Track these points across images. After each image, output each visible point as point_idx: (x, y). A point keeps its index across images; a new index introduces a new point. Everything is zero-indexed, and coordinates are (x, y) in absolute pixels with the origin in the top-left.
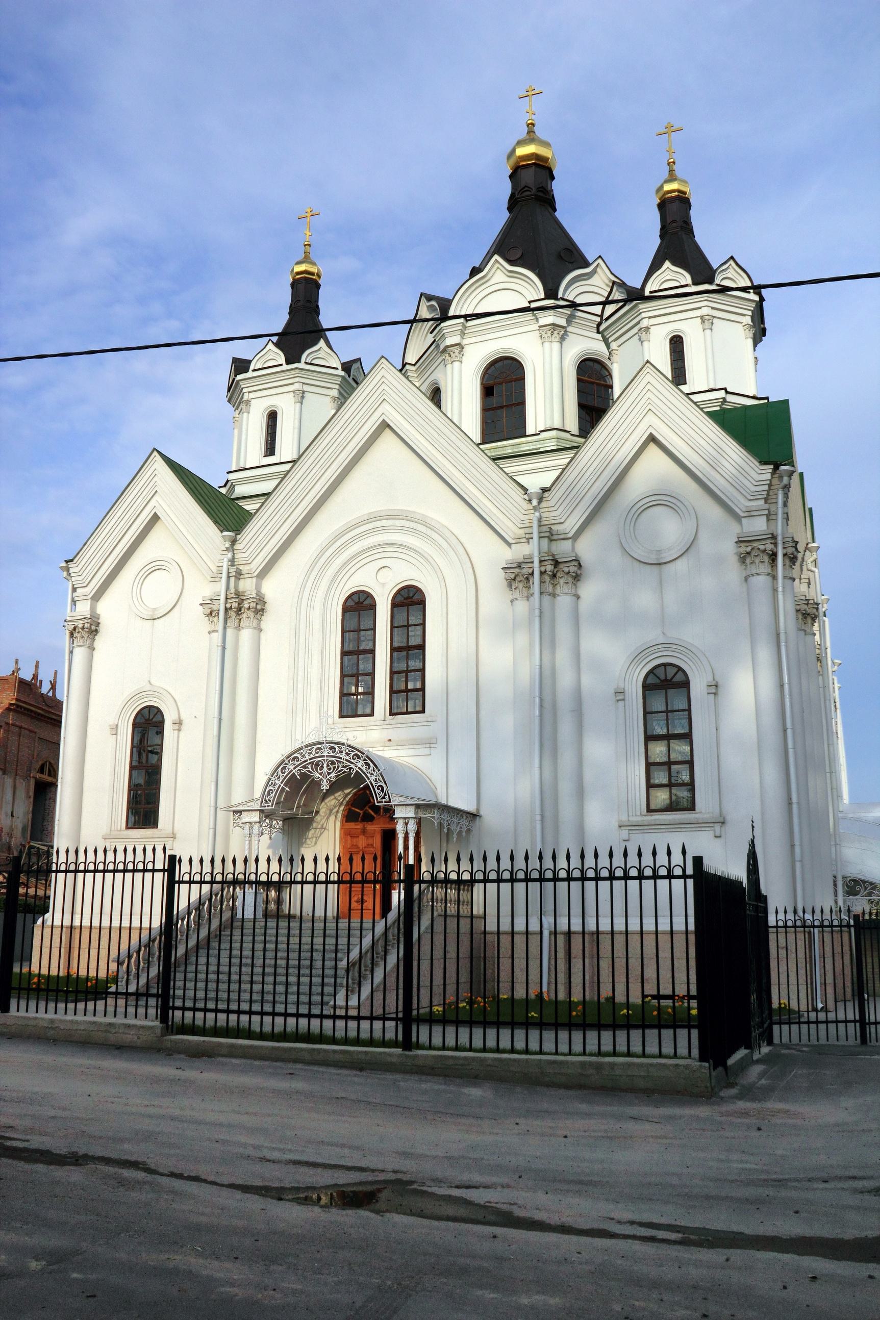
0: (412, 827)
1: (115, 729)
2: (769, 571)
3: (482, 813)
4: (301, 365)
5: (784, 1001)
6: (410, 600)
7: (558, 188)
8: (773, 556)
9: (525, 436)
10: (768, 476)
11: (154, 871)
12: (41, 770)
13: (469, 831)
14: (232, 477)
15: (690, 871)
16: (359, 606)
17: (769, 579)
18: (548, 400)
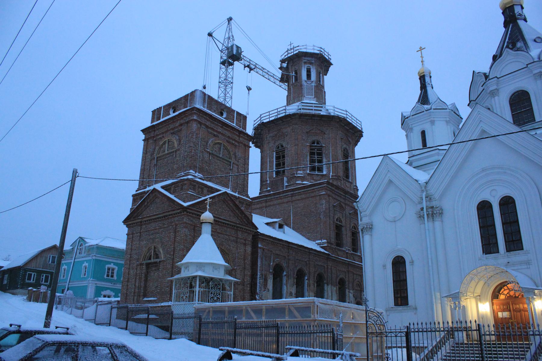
6: (508, 203)
14: (411, 159)
16: (484, 208)
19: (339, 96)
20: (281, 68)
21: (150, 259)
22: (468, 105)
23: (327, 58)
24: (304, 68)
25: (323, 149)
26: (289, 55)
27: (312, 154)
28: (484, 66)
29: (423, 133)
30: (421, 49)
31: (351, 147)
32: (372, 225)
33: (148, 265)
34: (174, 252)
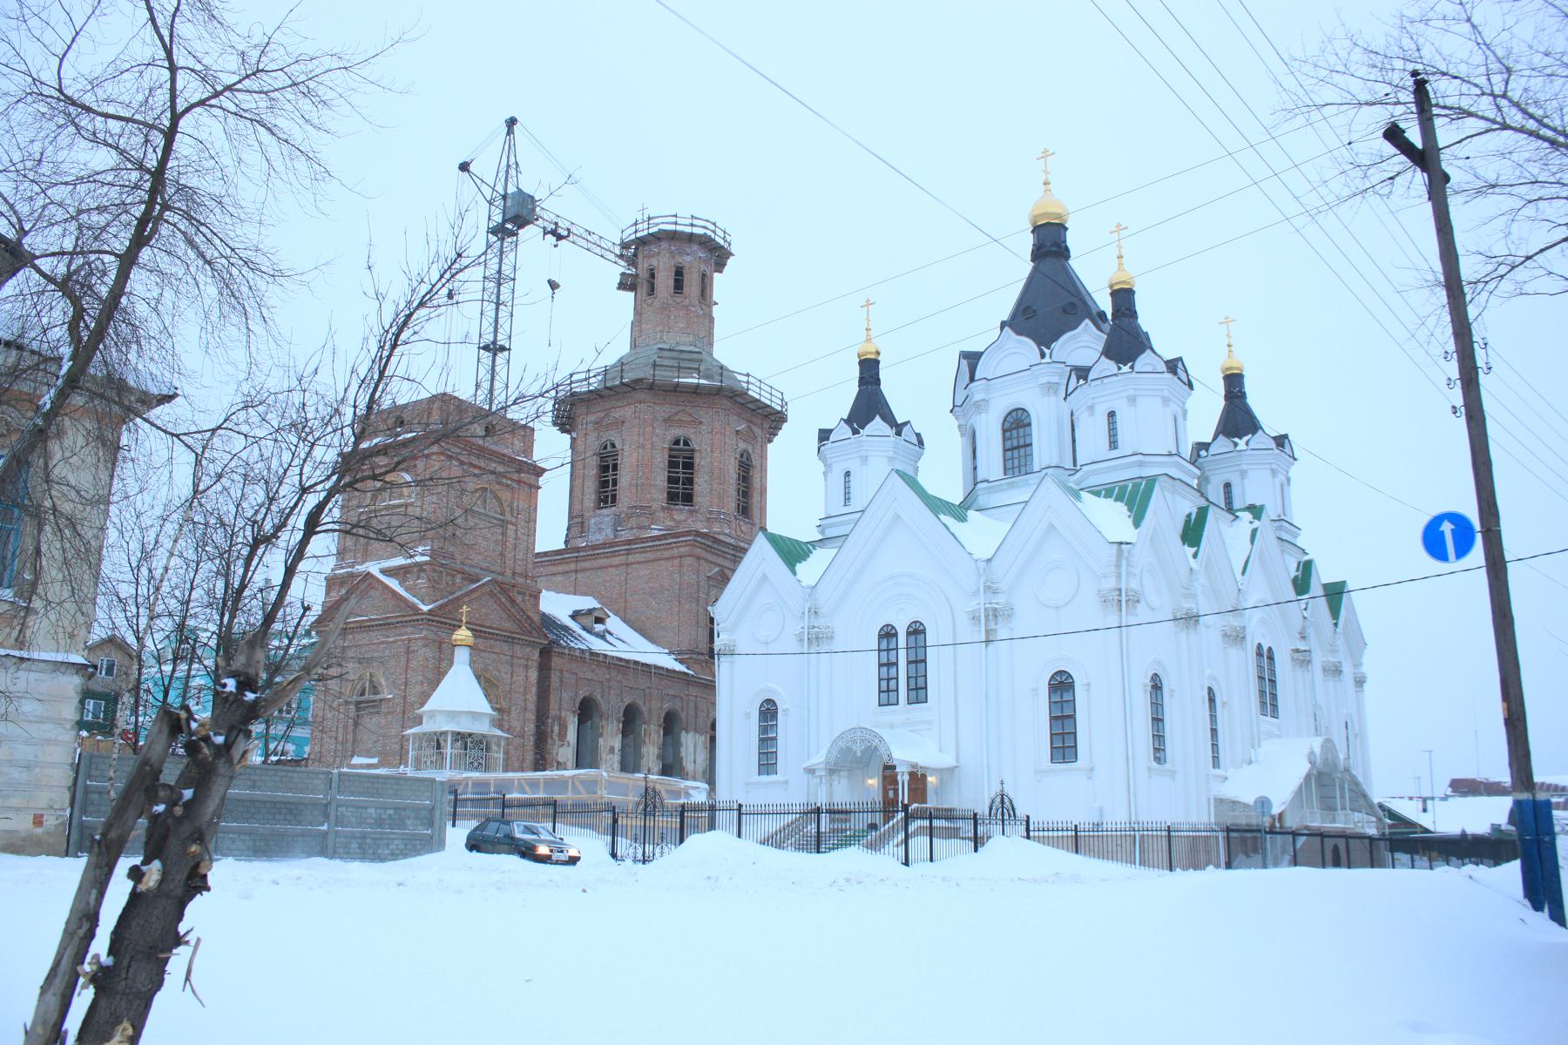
6: (916, 631)
7: (1072, 240)
16: (888, 634)
21: (363, 694)
23: (721, 242)
24: (672, 268)
25: (697, 455)
27: (672, 464)
33: (358, 703)
34: (406, 684)
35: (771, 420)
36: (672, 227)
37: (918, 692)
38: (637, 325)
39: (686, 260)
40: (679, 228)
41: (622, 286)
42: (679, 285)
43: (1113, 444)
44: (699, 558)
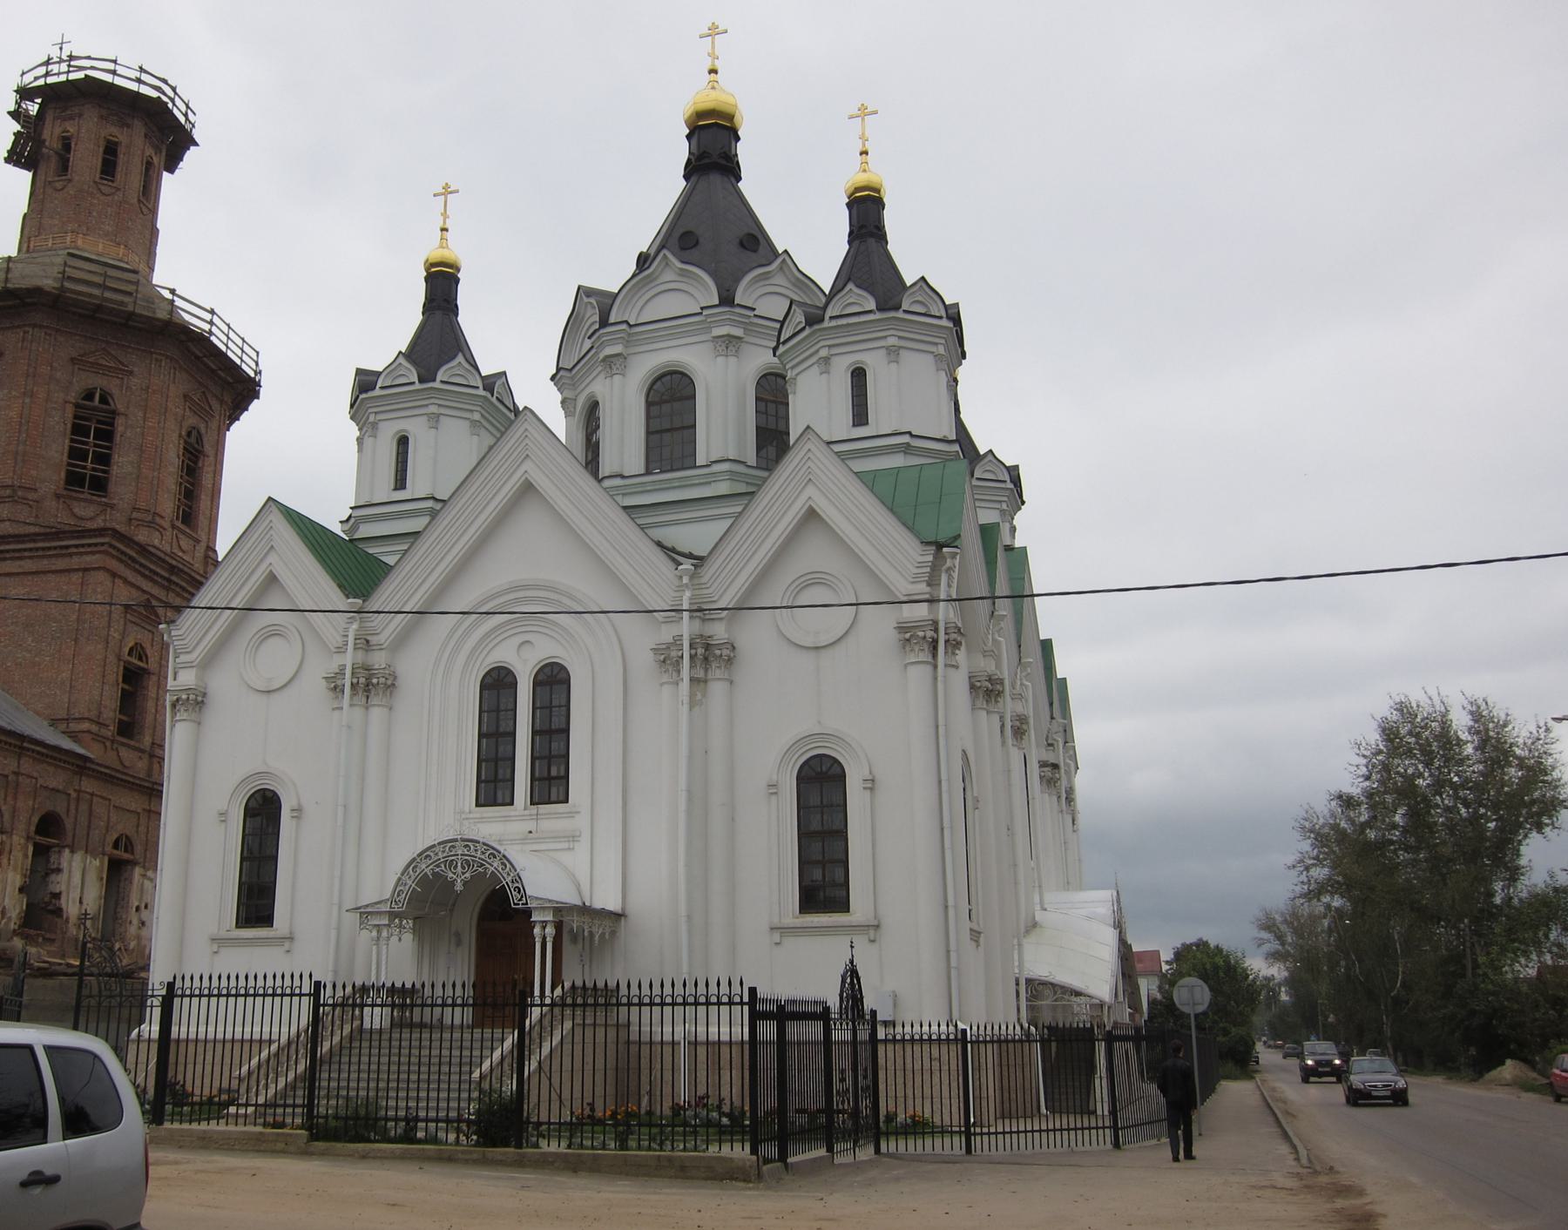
0: (550, 930)
1: (223, 816)
2: (930, 659)
3: (630, 911)
4: (437, 385)
5: (891, 1108)
6: (553, 680)
8: (934, 644)
9: (695, 467)
10: (930, 558)
11: (301, 995)
12: (116, 845)
13: (613, 933)
15: (746, 999)
16: (498, 684)
17: (929, 668)
18: (723, 424)
19: (202, 252)
20: (15, 115)
22: (553, 378)
23: (182, 119)
25: (120, 421)
26: (50, 80)
27: (78, 430)
28: (613, 275)
29: (403, 442)
30: (447, 191)
31: (214, 425)
32: (204, 695)
35: (235, 389)
36: (108, 78)
37: (551, 784)
38: (33, 225)
39: (121, 136)
40: (118, 81)
41: (14, 157)
42: (109, 167)
43: (860, 415)
44: (114, 575)
